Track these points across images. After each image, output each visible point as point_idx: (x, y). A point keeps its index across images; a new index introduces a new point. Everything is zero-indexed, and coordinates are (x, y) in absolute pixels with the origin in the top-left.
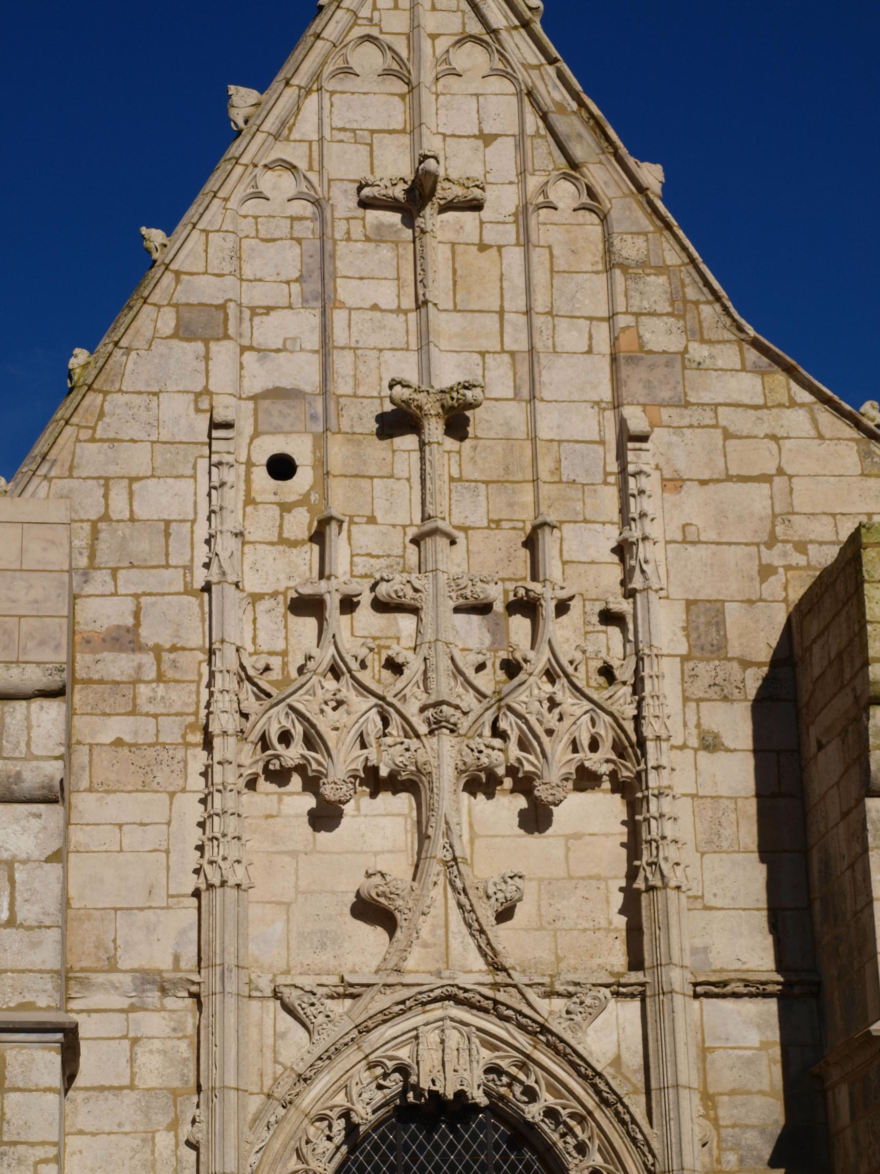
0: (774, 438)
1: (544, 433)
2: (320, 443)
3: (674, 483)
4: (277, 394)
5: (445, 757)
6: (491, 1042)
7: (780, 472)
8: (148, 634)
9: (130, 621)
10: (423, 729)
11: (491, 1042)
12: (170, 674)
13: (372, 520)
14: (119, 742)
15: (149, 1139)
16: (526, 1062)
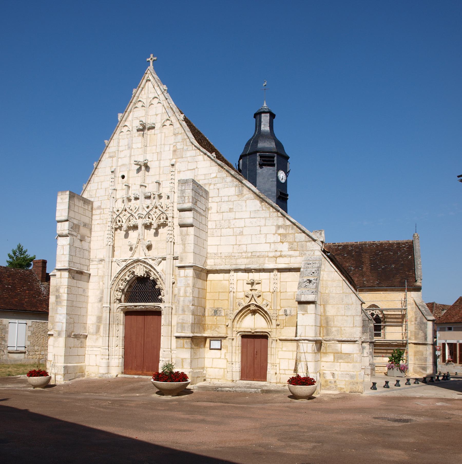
0: (197, 162)
1: (161, 166)
2: (128, 172)
3: (179, 172)
4: (123, 165)
5: (140, 222)
6: (146, 268)
7: (197, 168)
8: (102, 207)
9: (100, 205)
10: (137, 218)
11: (146, 268)
12: (105, 212)
13: (135, 184)
14: (98, 224)
15: (99, 283)
16: (151, 271)
